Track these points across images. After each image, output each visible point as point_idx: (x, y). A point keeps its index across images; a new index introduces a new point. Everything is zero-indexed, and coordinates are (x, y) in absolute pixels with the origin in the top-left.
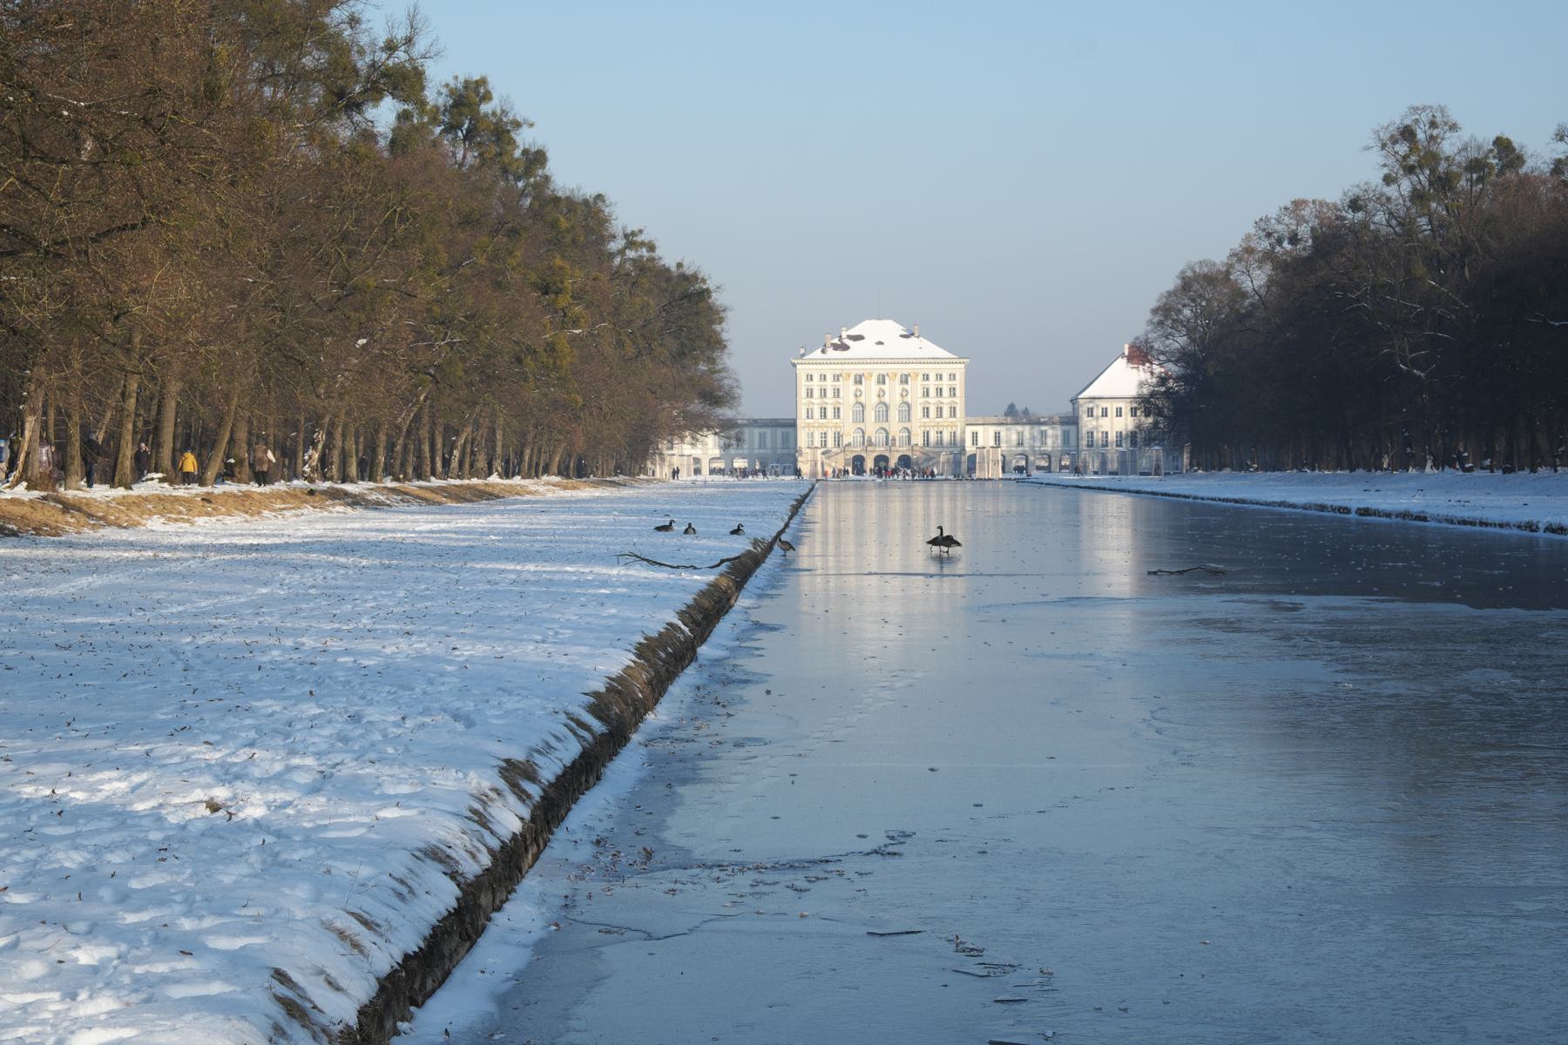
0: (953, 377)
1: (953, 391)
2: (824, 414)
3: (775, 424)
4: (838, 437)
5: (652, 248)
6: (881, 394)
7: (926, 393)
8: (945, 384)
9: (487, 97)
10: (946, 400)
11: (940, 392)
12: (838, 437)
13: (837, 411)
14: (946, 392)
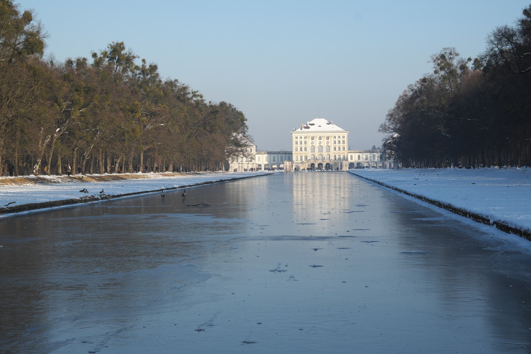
2: (301, 150)
3: (286, 153)
4: (306, 157)
5: (201, 97)
6: (320, 143)
8: (341, 139)
9: (123, 48)
10: (341, 145)
11: (339, 142)
12: (306, 157)
13: (306, 149)
14: (341, 142)
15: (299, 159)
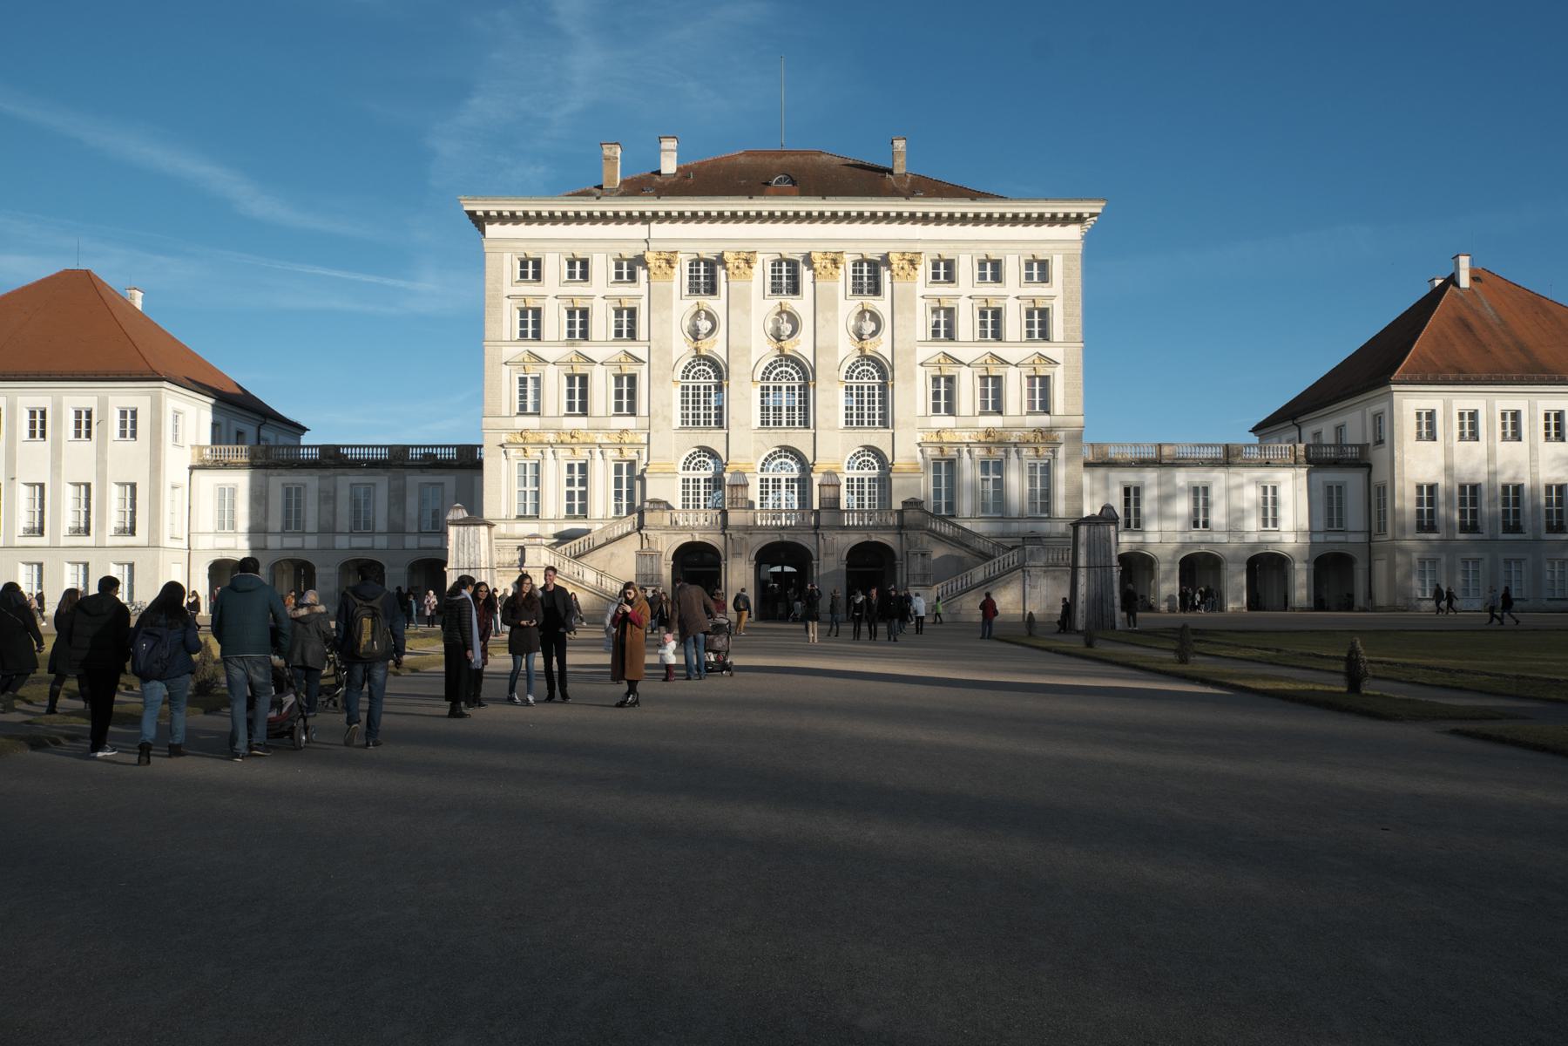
1: (1039, 323)
7: (945, 327)
8: (1013, 294)
10: (1016, 349)
14: (1014, 324)
15: (554, 501)
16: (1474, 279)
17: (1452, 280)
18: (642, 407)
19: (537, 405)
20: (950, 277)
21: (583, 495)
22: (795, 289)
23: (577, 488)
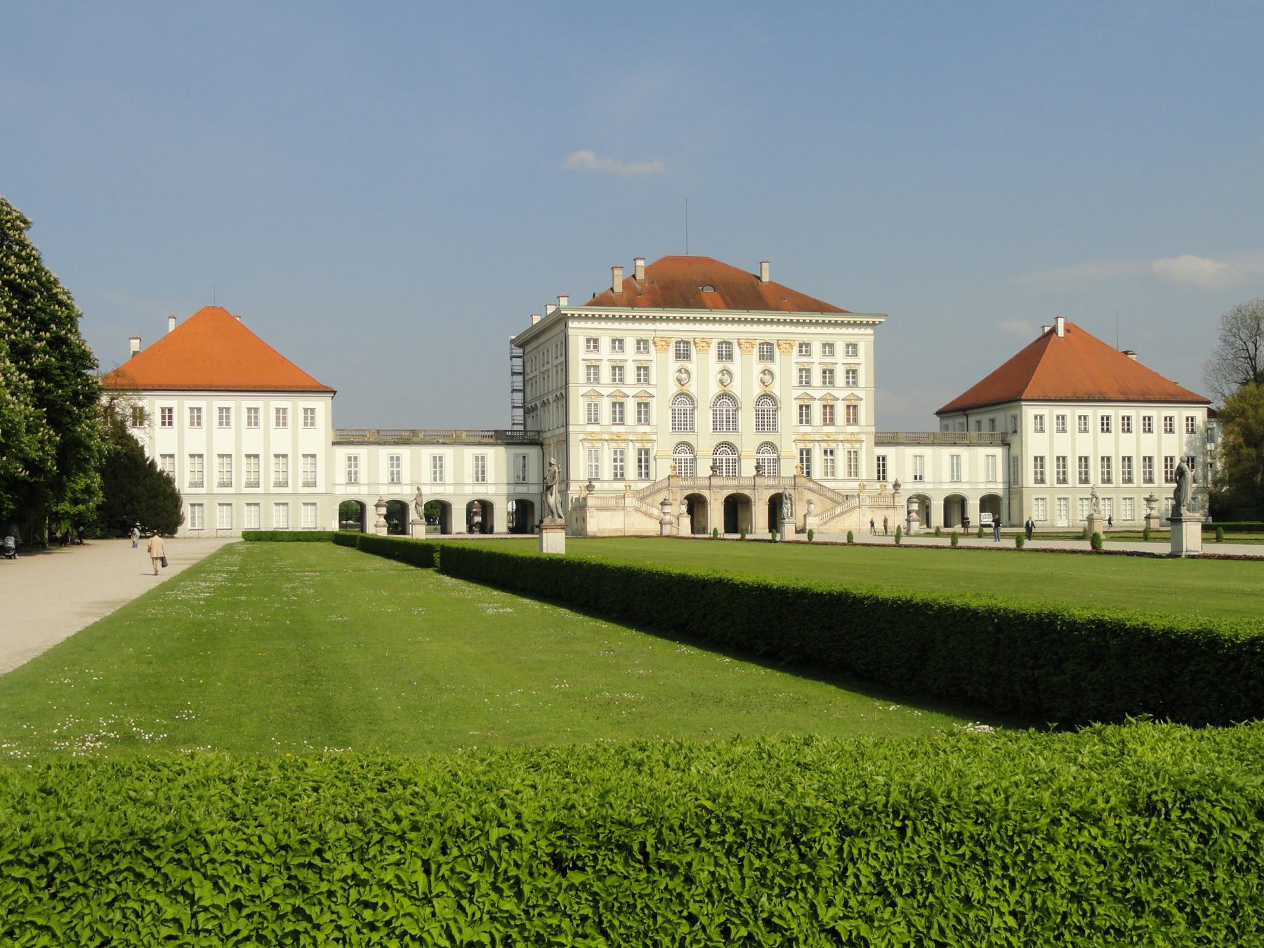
0: (852, 348)
8: (840, 360)
11: (828, 373)
13: (643, 407)
15: (607, 472)
16: (1067, 330)
17: (1054, 331)
18: (653, 420)
19: (596, 419)
20: (808, 353)
21: (622, 468)
22: (730, 357)
23: (619, 464)
